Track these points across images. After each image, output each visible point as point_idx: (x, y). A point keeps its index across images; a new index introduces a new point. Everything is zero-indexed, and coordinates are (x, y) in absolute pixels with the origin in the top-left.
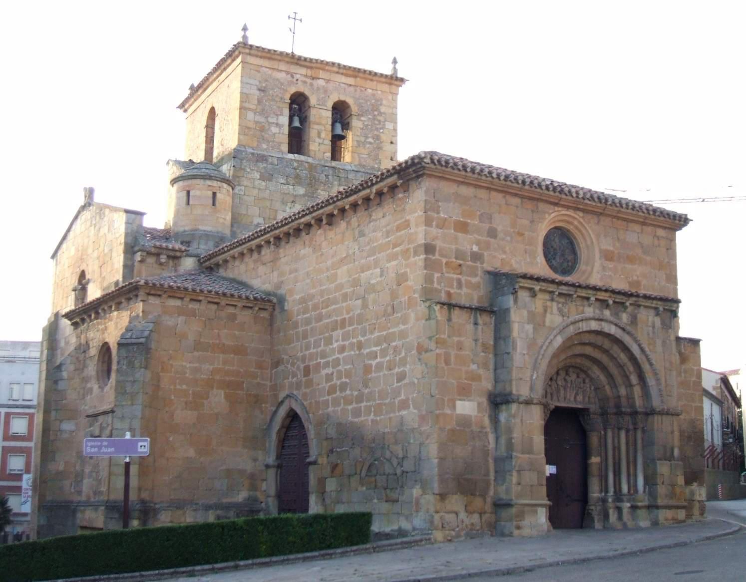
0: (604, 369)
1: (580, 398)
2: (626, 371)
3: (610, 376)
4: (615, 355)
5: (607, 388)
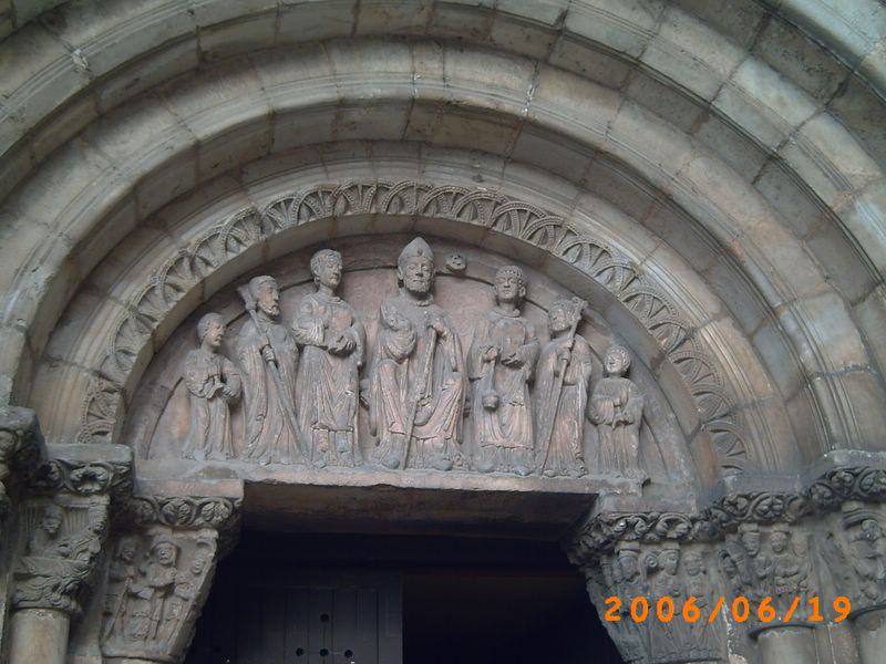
0: (655, 208)
1: (508, 428)
2: (813, 178)
3: (711, 253)
4: (701, 87)
5: (719, 341)
